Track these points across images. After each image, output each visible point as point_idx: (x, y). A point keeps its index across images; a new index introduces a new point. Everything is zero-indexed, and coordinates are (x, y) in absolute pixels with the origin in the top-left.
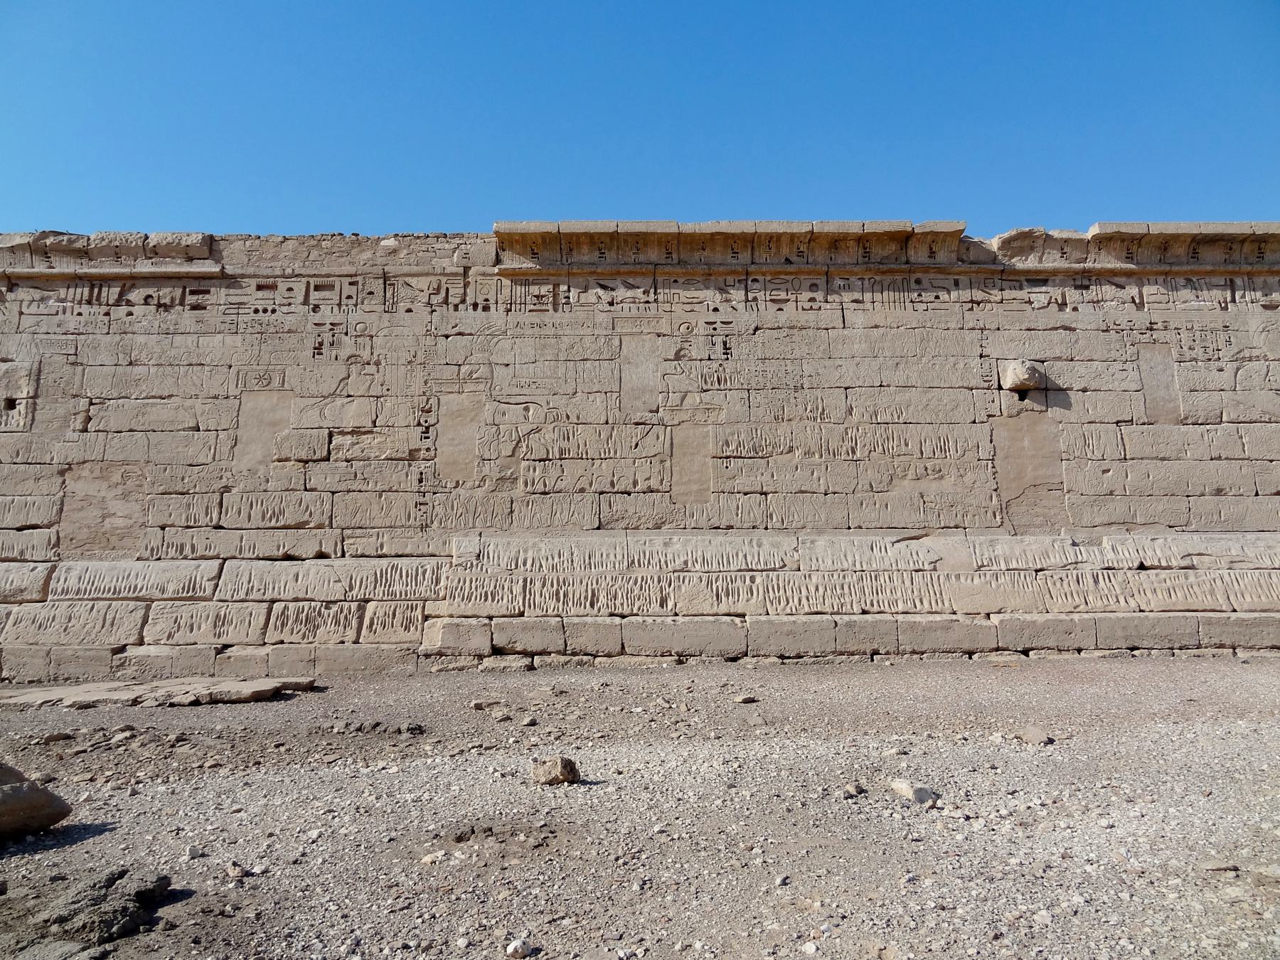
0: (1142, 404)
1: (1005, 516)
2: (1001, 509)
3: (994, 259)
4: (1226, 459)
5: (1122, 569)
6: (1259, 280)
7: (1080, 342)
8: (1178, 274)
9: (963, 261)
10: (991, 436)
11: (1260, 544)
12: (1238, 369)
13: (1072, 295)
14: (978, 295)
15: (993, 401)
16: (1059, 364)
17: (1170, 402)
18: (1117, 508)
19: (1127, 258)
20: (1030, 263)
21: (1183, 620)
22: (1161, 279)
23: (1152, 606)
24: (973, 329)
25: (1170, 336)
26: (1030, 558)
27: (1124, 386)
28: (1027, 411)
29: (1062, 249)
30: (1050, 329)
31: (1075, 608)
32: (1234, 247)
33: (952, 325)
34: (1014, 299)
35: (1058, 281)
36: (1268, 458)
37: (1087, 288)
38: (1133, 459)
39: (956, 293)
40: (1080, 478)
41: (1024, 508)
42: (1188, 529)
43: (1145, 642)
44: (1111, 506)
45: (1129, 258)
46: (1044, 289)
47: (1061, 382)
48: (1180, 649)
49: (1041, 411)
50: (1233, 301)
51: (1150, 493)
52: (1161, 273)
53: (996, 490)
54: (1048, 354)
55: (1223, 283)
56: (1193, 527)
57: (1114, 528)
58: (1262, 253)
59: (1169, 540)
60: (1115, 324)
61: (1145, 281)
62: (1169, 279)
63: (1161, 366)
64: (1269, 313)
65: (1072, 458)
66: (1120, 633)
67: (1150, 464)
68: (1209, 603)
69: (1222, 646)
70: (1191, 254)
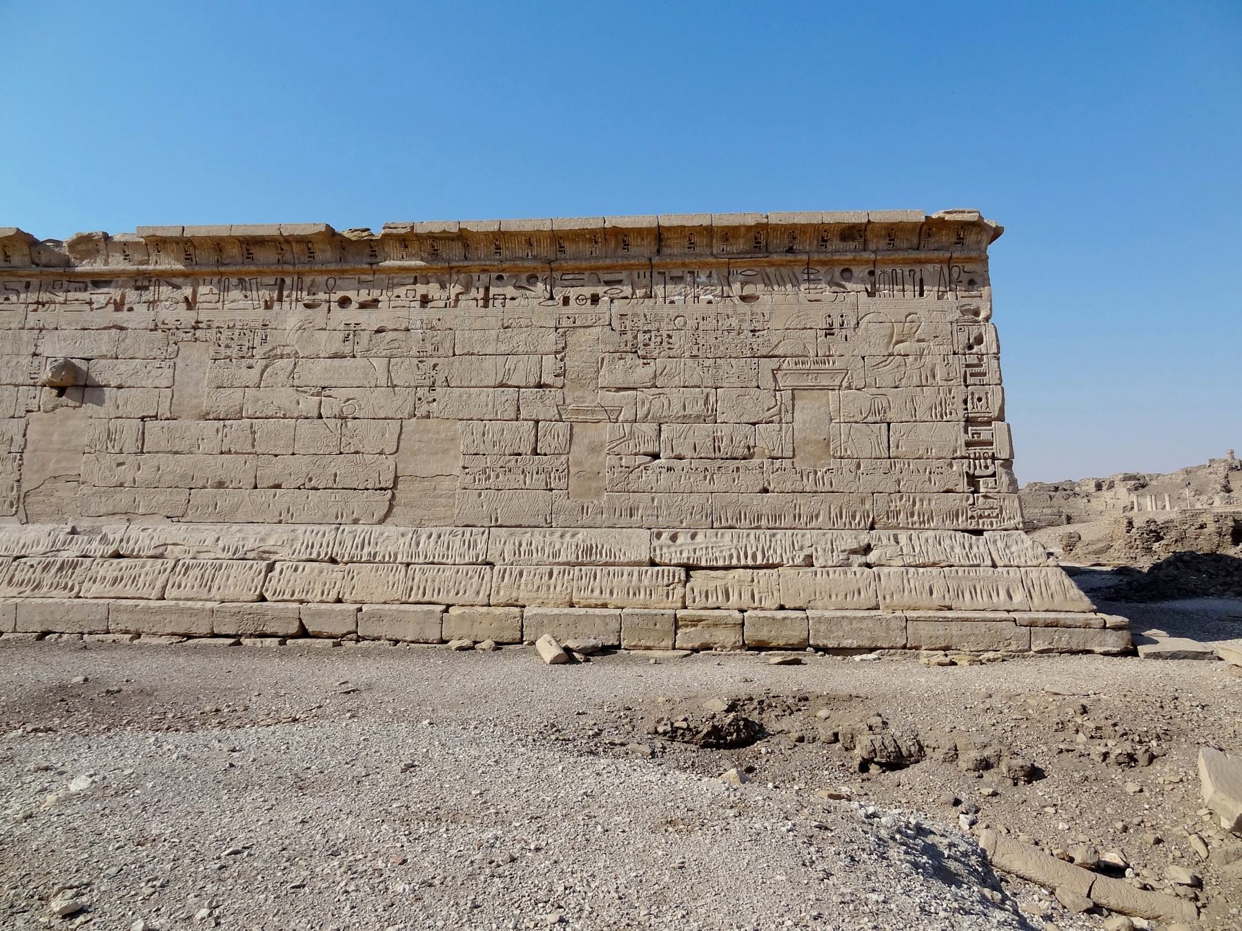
0: (169, 400)
1: (21, 505)
2: (19, 498)
3: (68, 264)
4: (236, 453)
5: (96, 557)
6: (308, 280)
7: (127, 340)
8: (233, 274)
9: (37, 265)
10: (25, 430)
11: (238, 535)
12: (266, 367)
13: (132, 295)
14: (45, 297)
15: (34, 398)
16: (103, 362)
17: (195, 398)
18: (123, 499)
19: (186, 259)
20: (96, 266)
21: (94, 607)
22: (215, 279)
23: (88, 595)
24: (33, 329)
25: (212, 334)
26: (21, 545)
27: (157, 382)
28: (62, 406)
29: (125, 252)
30: (105, 329)
31: (20, 593)
32: (284, 247)
33: (13, 326)
34: (77, 300)
35: (120, 283)
36: (273, 452)
37: (146, 288)
38: (149, 453)
39: (25, 295)
40: (96, 469)
41: (40, 498)
42: (184, 520)
43: (59, 627)
44: (118, 497)
45: (188, 258)
46: (105, 290)
47: (100, 380)
48: (90, 633)
49: (75, 407)
50: (280, 299)
51: (157, 485)
52: (214, 274)
53: (18, 481)
54: (95, 353)
55: (273, 283)
56: (188, 519)
57: (117, 517)
58: (313, 253)
59: (158, 530)
60: (163, 323)
61: (201, 282)
62: (223, 280)
63: (196, 364)
64: (309, 311)
65: (92, 451)
66: (37, 618)
67: (162, 457)
68: (144, 592)
69: (127, 632)
70: (246, 255)
